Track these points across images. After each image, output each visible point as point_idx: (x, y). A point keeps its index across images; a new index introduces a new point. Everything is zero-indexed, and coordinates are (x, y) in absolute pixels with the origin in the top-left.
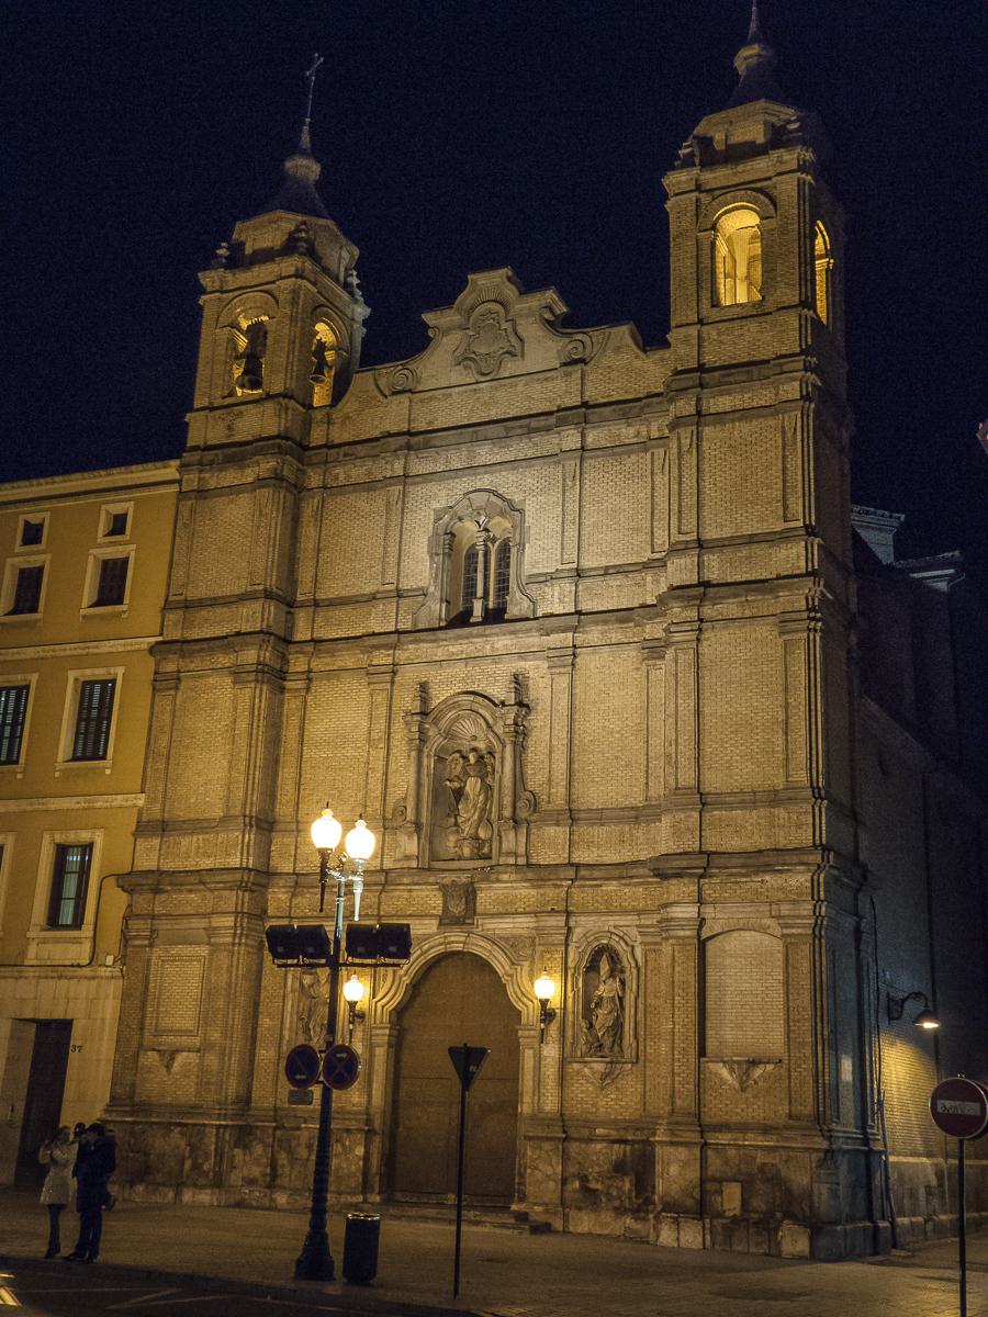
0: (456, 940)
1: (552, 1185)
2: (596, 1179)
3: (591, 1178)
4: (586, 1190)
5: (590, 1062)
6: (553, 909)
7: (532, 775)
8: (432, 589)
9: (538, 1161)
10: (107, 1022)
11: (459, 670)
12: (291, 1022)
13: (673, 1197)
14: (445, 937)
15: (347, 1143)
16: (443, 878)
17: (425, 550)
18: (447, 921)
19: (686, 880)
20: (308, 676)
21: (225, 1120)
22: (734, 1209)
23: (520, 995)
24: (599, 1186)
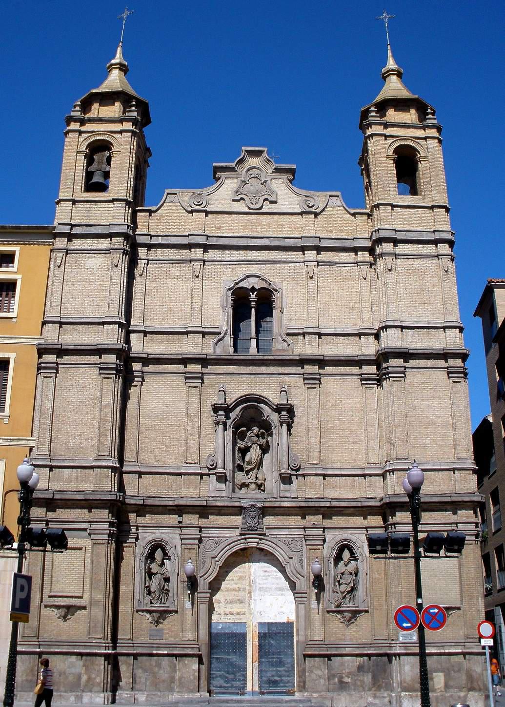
0: (253, 543)
1: (322, 681)
2: (346, 676)
3: (344, 676)
4: (341, 682)
13: (408, 684)
15: (186, 662)
17: (219, 304)
21: (109, 650)
24: (349, 680)
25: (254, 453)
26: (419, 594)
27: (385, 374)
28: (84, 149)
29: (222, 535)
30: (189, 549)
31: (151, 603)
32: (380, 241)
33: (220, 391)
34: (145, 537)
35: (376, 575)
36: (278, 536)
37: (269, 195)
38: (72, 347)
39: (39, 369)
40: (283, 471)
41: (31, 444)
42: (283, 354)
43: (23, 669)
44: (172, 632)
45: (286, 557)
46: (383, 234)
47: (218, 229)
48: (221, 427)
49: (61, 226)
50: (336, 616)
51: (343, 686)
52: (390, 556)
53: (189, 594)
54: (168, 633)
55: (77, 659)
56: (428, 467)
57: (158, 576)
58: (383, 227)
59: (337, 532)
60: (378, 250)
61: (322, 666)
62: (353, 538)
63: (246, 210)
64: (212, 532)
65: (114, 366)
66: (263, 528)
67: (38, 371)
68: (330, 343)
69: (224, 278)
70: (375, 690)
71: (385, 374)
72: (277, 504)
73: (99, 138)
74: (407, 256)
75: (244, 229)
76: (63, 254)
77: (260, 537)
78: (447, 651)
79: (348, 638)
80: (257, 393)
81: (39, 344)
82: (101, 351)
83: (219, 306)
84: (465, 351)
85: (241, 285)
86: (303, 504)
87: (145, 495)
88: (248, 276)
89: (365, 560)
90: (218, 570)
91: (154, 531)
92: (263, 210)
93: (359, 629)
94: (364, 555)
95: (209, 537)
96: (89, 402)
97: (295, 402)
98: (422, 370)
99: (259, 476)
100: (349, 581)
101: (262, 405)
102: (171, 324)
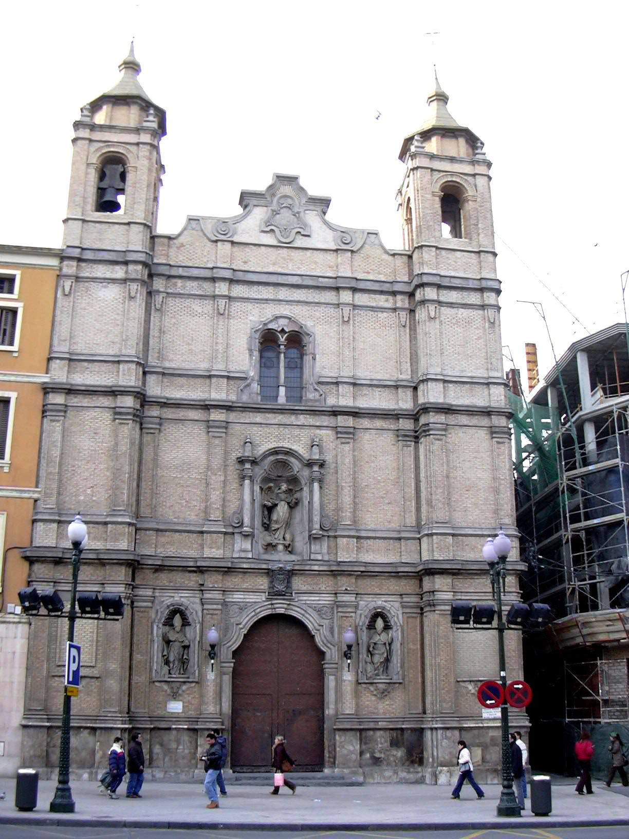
3: (376, 751)
5: (376, 683)
6: (346, 589)
7: (327, 503)
8: (252, 374)
9: (343, 743)
10: (17, 655)
11: (275, 431)
12: (157, 658)
14: (272, 604)
16: (273, 566)
18: (274, 594)
19: (445, 576)
20: (161, 420)
21: (125, 724)
22: (478, 761)
23: (325, 642)
24: (382, 756)
25: (282, 510)
26: (503, 668)
27: (425, 431)
28: (95, 162)
29: (248, 600)
30: (212, 614)
31: (170, 673)
32: (422, 285)
33: (246, 443)
34: (163, 601)
35: (411, 646)
36: (308, 602)
37: (302, 228)
38: (83, 388)
39: (44, 412)
40: (314, 532)
41: (36, 496)
42: (315, 404)
43: (30, 744)
44: (191, 704)
45: (316, 625)
46: (425, 279)
47: (245, 262)
48: (247, 482)
49: (70, 250)
51: (376, 761)
52: (472, 627)
53: (212, 664)
54: (187, 706)
55: (89, 734)
56: (469, 533)
57: (177, 644)
58: (426, 271)
59: (369, 598)
60: (418, 296)
61: (354, 741)
62: (388, 606)
63: (275, 243)
64: (235, 596)
65: (131, 410)
66: (291, 593)
67: (43, 413)
68: (365, 394)
69: (251, 318)
70: (408, 766)
71: (425, 431)
72: (307, 568)
73: (112, 149)
74: (451, 305)
75: (274, 264)
76: (72, 282)
77: (288, 603)
78: (485, 725)
79: (381, 711)
80: (286, 446)
81: (45, 383)
82: (117, 393)
83: (245, 348)
84: (510, 411)
85: (270, 326)
86: (334, 568)
87: (162, 555)
88: (277, 318)
89: (400, 630)
90: (242, 638)
91: (173, 595)
92: (296, 245)
93: (392, 703)
94: (398, 624)
95: (233, 602)
96: (102, 450)
97: (329, 458)
98: (465, 429)
99: (288, 536)
100: (382, 651)
101: (292, 460)
102: (192, 366)
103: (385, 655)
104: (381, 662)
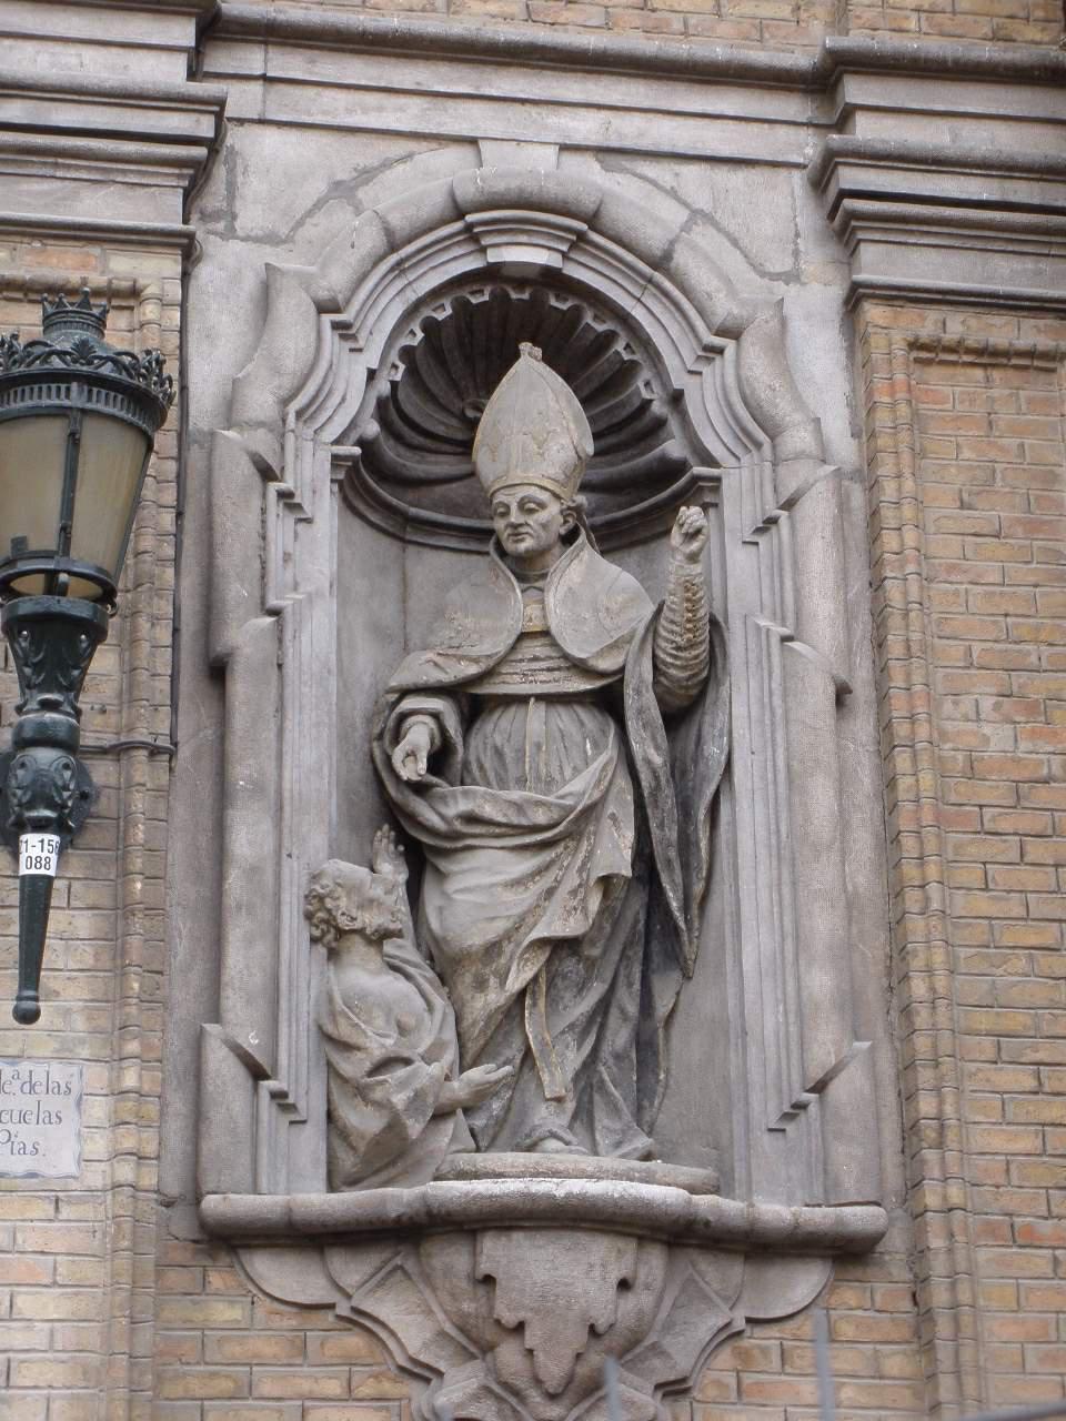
50: (358, 1320)
89: (818, 510)
103: (614, 850)
104: (560, 947)
